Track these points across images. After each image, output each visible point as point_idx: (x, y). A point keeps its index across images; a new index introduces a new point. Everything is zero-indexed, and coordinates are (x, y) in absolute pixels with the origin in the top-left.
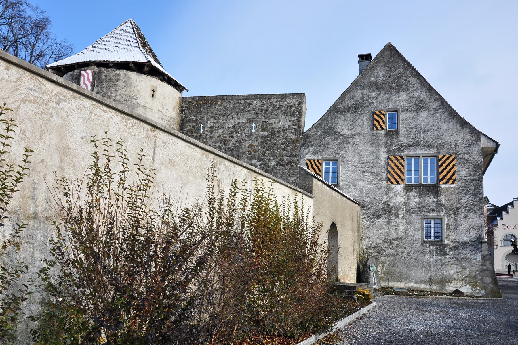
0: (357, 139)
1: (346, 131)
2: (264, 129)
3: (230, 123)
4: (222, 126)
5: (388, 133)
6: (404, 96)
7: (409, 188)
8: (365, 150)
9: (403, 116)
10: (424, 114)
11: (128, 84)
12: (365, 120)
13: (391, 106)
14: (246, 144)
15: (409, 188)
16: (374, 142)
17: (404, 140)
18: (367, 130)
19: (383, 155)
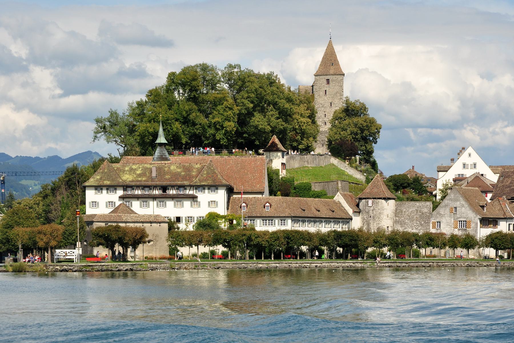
0: (446, 215)
1: (443, 213)
2: (420, 212)
3: (411, 210)
4: (408, 211)
5: (454, 214)
6: (458, 203)
7: (459, 230)
8: (448, 218)
9: (458, 209)
10: (463, 208)
11: (382, 203)
12: (448, 210)
13: (455, 206)
14: (415, 217)
15: (459, 230)
16: (450, 216)
17: (458, 216)
18: (448, 213)
19: (453, 220)
